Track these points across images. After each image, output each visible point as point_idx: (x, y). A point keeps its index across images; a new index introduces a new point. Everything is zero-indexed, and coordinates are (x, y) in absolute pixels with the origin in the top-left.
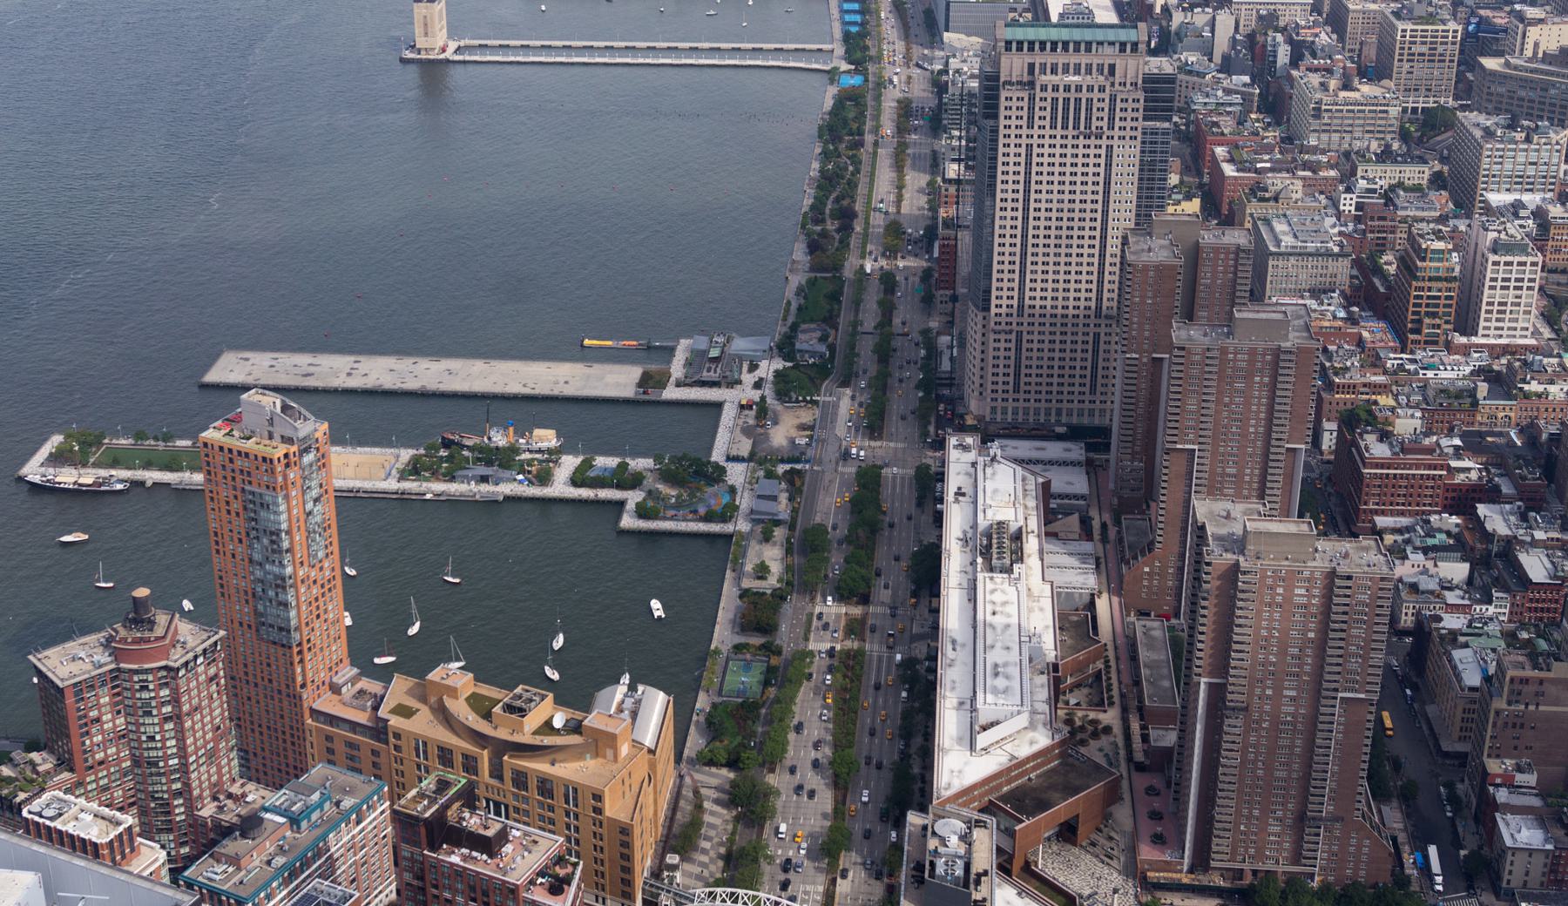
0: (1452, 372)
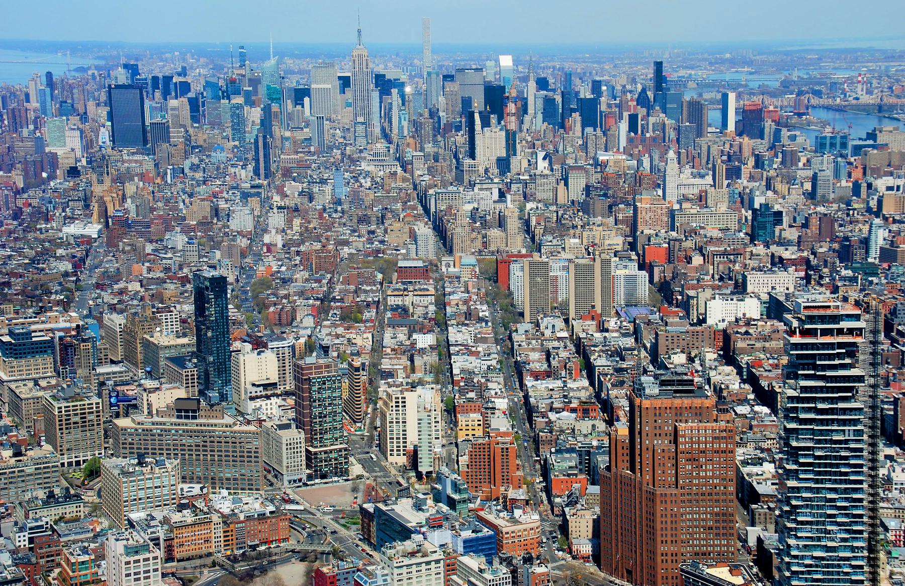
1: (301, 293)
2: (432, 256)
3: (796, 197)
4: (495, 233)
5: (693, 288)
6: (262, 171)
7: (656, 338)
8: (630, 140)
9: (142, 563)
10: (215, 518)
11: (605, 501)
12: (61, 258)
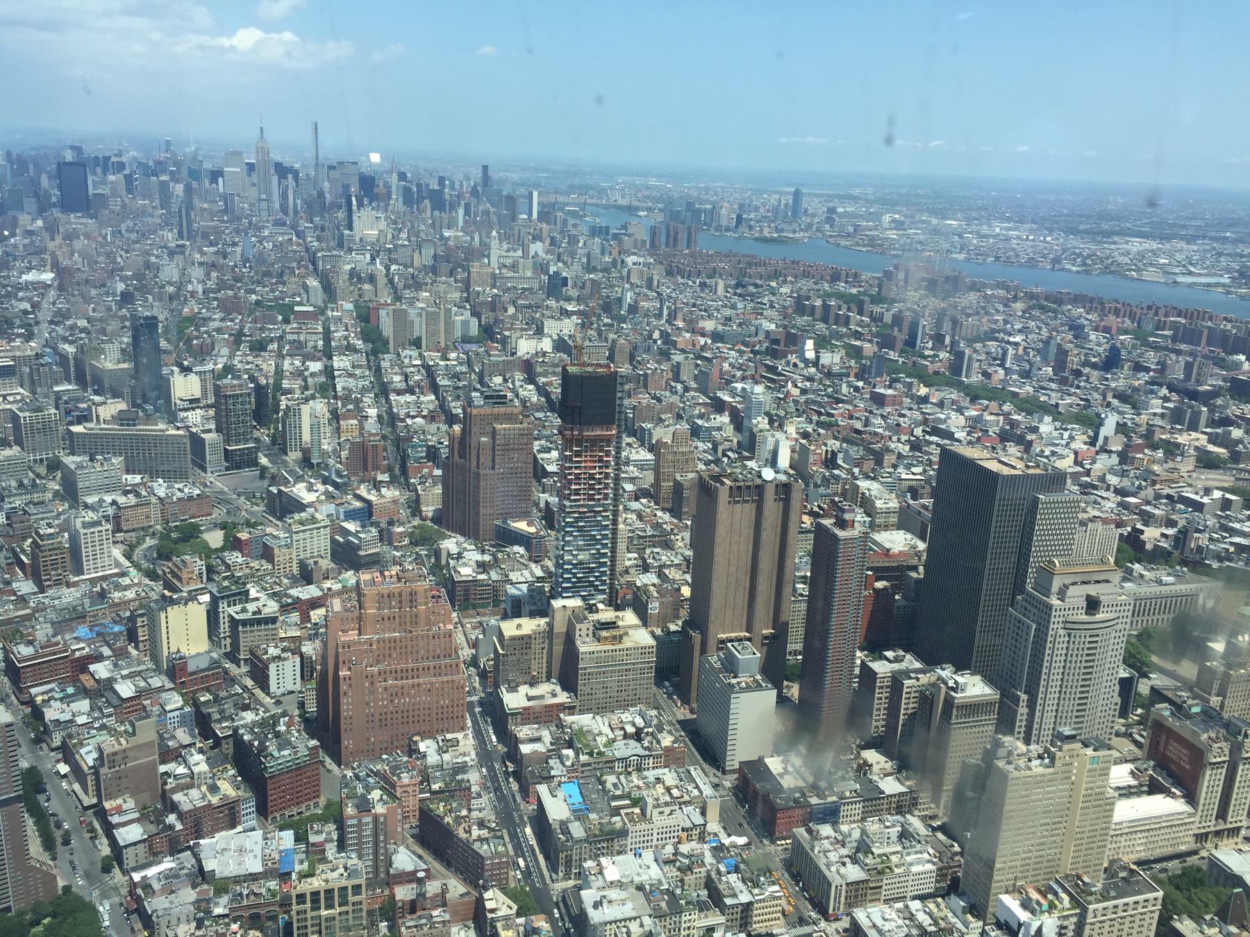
0: (69, 596)
1: (219, 330)
2: (321, 304)
3: (576, 267)
4: (367, 287)
5: (509, 329)
6: (185, 235)
7: (483, 366)
8: (465, 222)
9: (97, 534)
10: (154, 500)
11: (446, 482)
12: (22, 300)
